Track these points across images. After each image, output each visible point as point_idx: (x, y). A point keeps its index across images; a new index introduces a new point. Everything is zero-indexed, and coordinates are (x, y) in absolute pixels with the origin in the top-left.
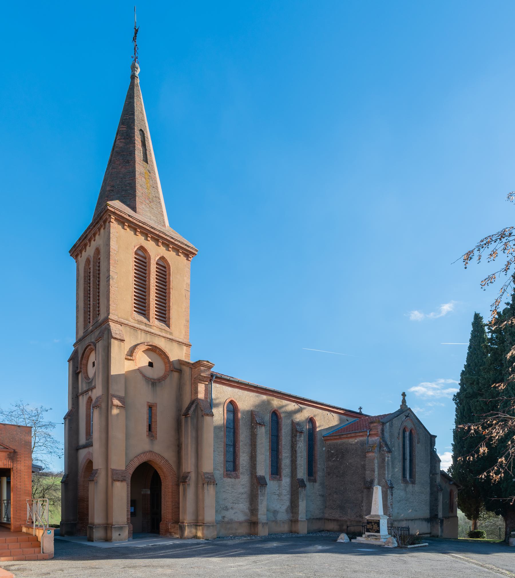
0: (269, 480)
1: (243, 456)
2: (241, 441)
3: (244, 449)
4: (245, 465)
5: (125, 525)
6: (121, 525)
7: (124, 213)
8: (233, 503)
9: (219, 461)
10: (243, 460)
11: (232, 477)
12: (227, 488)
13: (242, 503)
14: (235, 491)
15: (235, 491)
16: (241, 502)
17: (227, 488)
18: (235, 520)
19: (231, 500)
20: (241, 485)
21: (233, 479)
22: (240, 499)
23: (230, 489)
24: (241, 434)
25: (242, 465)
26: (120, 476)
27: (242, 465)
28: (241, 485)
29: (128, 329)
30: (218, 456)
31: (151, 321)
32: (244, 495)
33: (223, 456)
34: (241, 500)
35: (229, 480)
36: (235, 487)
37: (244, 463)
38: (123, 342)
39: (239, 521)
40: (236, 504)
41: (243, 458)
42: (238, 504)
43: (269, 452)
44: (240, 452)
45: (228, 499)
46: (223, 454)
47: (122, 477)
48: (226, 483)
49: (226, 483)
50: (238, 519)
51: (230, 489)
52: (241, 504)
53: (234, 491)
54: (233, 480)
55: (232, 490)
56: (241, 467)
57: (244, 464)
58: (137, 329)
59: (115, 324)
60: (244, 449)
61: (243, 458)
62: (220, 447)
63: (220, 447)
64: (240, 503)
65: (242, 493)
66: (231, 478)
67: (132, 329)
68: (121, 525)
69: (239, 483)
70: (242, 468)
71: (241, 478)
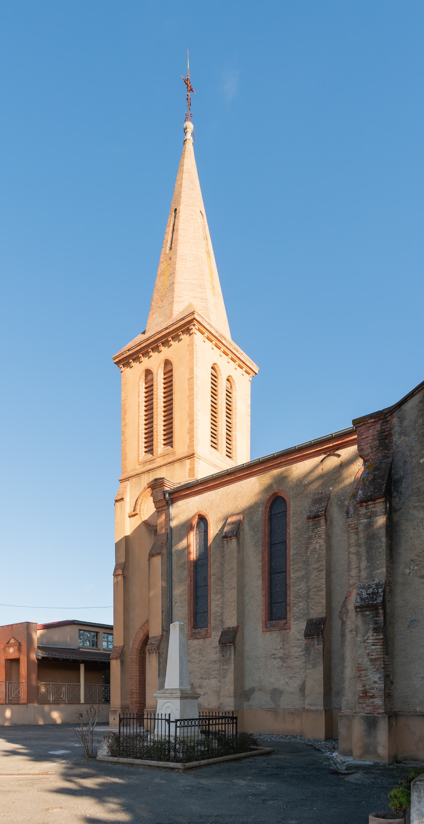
0: (261, 632)
1: (216, 599)
2: (213, 575)
3: (217, 587)
4: (219, 614)
5: (119, 708)
6: (116, 708)
7: (150, 338)
8: (202, 679)
9: (182, 616)
10: (217, 606)
11: (199, 637)
12: (193, 655)
13: (214, 678)
14: (204, 659)
15: (204, 659)
16: (213, 677)
17: (193, 655)
18: (204, 706)
19: (198, 673)
20: (213, 648)
21: (202, 639)
22: (212, 671)
23: (197, 656)
24: (212, 564)
25: (215, 615)
26: (116, 653)
27: (215, 615)
28: (213, 648)
29: (134, 479)
30: (181, 608)
31: (155, 453)
32: (217, 664)
33: (187, 607)
34: (213, 673)
35: (196, 642)
36: (204, 652)
37: (218, 610)
38: (123, 500)
39: (210, 707)
40: (205, 679)
41: (216, 602)
42: (209, 679)
43: (261, 579)
44: (212, 594)
45: (194, 672)
46: (187, 604)
47: (117, 654)
48: (192, 647)
49: (192, 647)
50: (209, 704)
51: (197, 656)
52: (214, 679)
53: (203, 659)
54: (201, 641)
55: (200, 657)
56: (212, 619)
57: (218, 612)
58: (141, 474)
59: (125, 482)
60: (217, 587)
61: (216, 602)
62: (184, 595)
63: (184, 595)
64: (211, 678)
65: (215, 661)
66: (198, 639)
67: (137, 478)
68: (116, 708)
69: (211, 645)
70: (214, 620)
71: (213, 637)
